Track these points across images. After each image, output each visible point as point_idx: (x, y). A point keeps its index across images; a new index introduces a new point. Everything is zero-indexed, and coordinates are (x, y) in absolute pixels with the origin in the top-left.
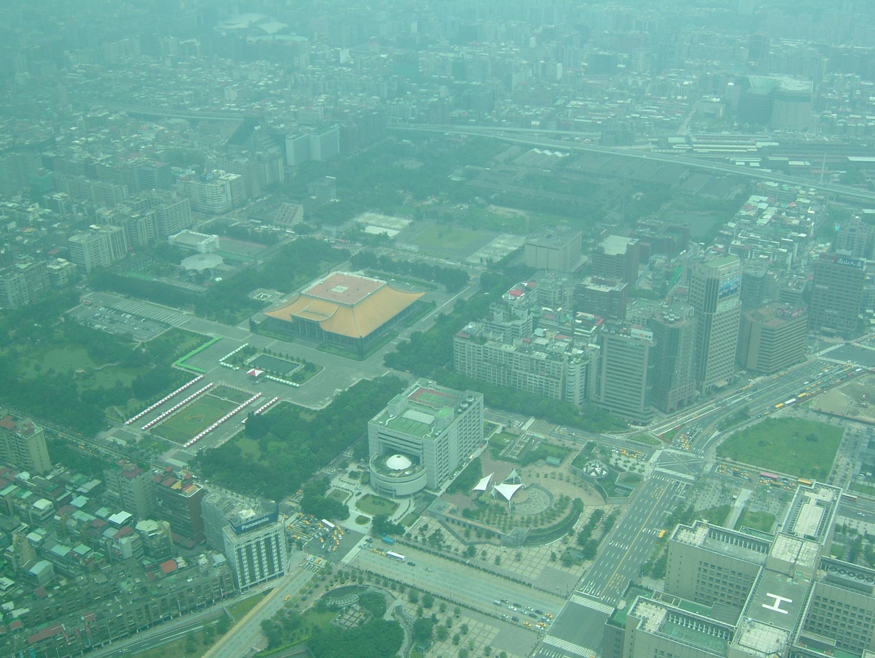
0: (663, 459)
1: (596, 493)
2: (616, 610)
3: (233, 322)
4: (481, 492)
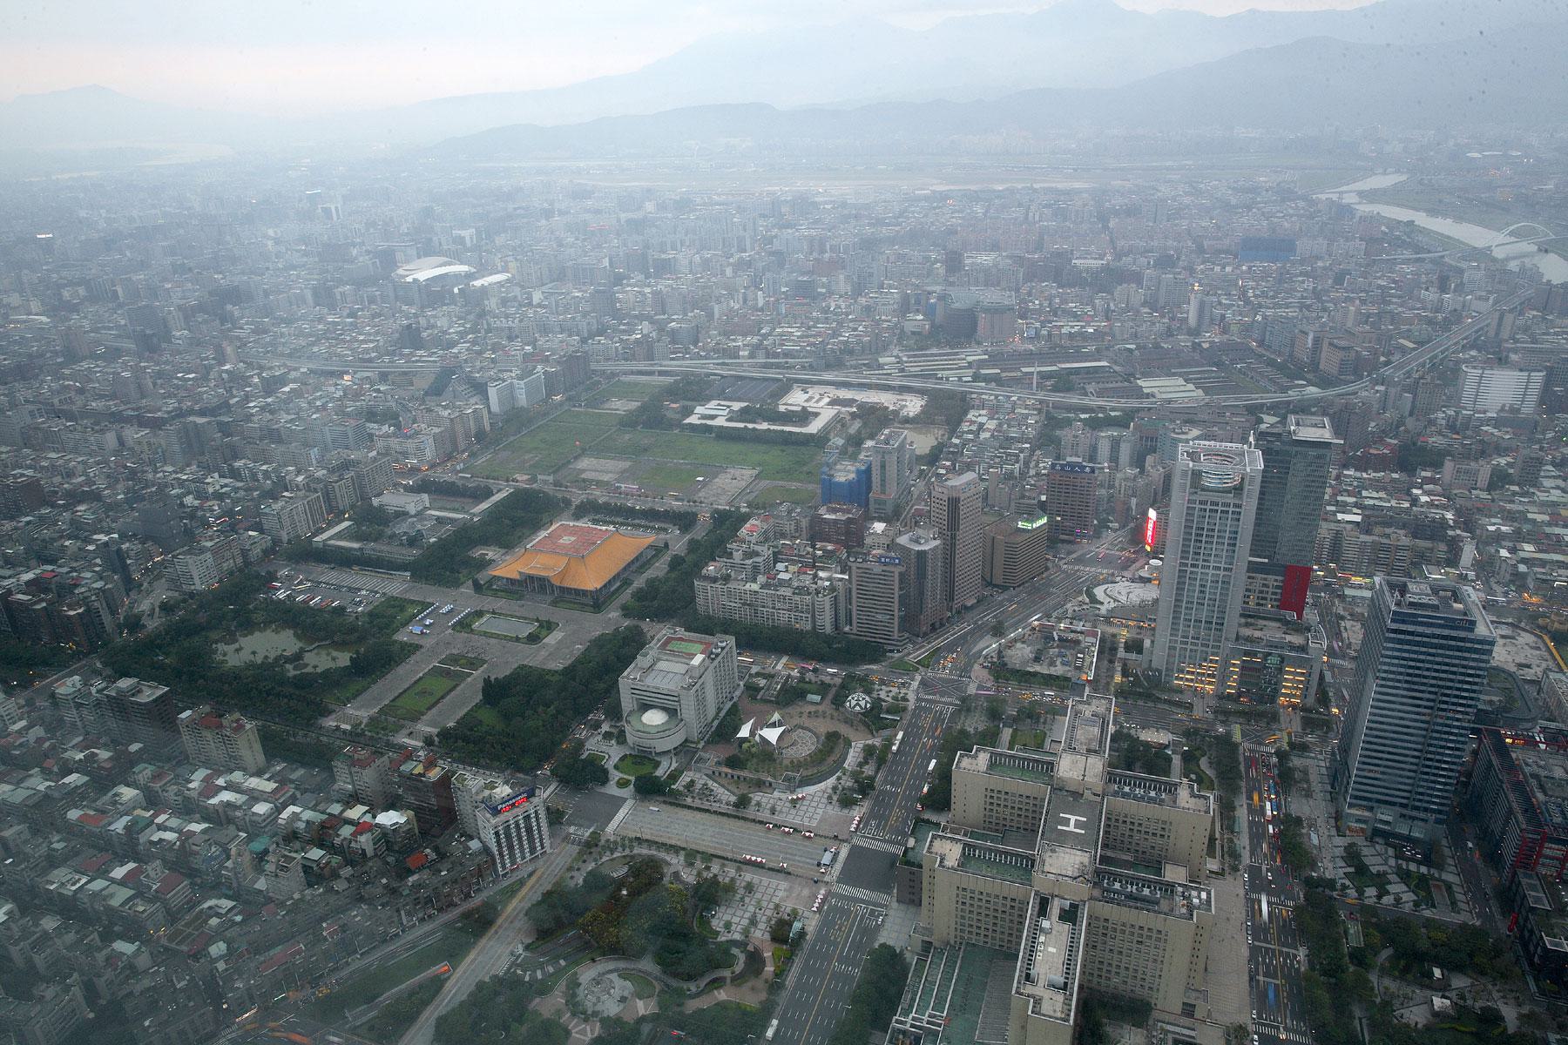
0: (923, 683)
1: (862, 728)
3: (456, 584)
4: (744, 740)
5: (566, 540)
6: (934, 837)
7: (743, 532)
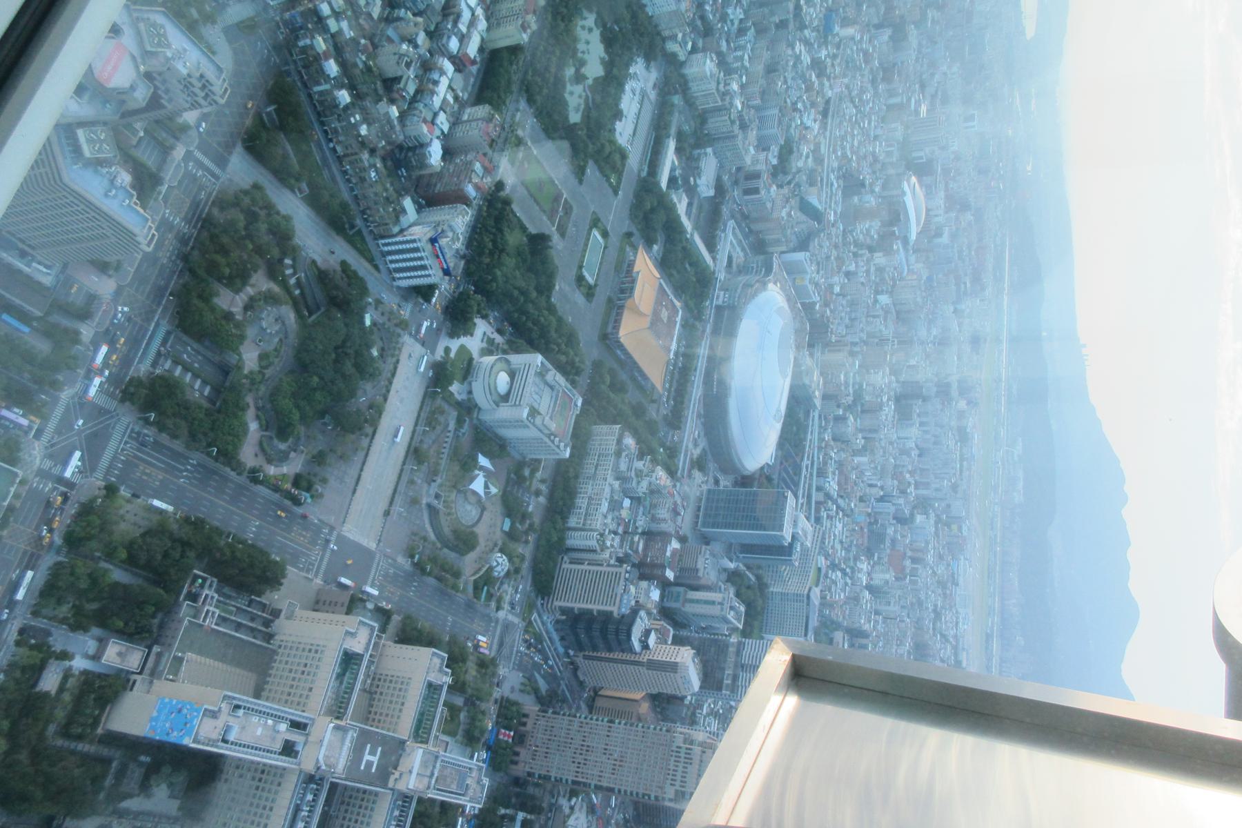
0: (507, 627)
2: (365, 601)
4: (475, 460)
5: (665, 314)
6: (372, 628)
7: (661, 473)
